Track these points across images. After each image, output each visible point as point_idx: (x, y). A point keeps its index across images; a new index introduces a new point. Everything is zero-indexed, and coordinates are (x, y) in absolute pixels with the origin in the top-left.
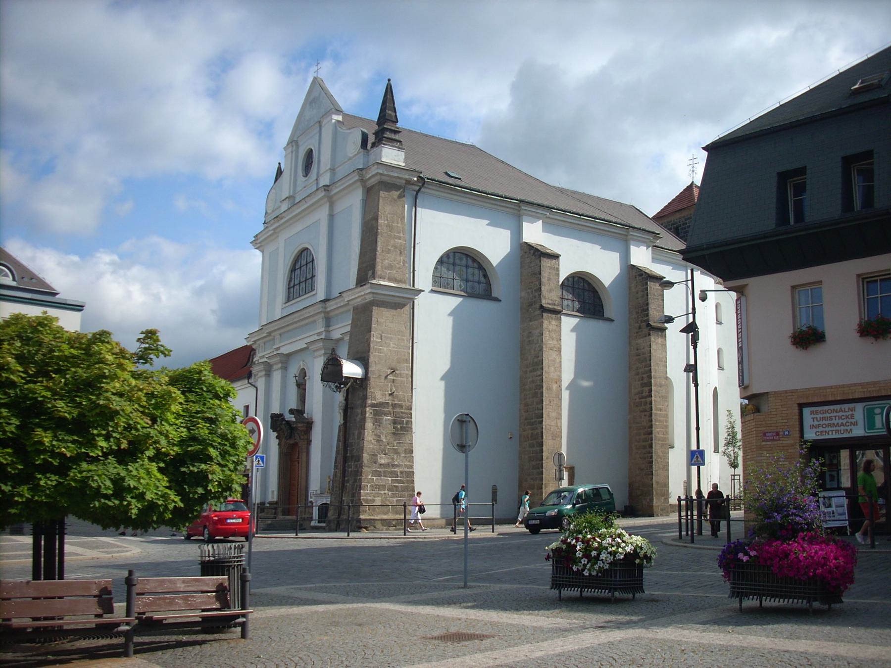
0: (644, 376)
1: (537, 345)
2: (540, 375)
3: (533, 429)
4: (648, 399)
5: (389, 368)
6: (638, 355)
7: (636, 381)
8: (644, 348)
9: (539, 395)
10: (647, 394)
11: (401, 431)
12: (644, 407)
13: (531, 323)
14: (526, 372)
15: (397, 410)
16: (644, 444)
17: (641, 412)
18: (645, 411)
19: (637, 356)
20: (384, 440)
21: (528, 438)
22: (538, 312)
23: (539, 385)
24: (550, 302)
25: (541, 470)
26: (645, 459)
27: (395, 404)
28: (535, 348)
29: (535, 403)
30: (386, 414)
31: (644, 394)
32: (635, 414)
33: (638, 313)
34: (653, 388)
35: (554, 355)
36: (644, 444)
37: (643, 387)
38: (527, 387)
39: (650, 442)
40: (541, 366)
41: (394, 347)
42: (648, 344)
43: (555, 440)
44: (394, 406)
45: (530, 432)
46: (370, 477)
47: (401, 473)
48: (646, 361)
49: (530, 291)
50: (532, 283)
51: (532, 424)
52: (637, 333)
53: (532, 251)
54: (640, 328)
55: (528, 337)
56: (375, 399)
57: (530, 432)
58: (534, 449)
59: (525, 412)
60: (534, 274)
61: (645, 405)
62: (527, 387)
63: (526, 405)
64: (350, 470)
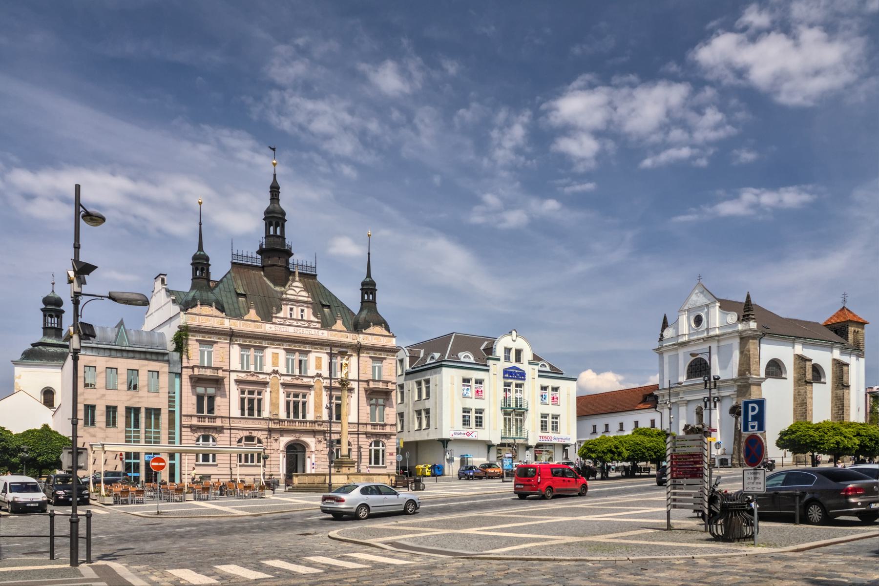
34: (845, 411)
35: (810, 400)
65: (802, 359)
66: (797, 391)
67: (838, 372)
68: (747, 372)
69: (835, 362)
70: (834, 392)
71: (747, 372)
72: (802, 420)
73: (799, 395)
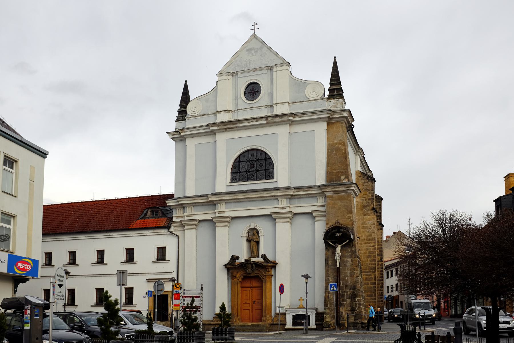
1: (370, 230)
2: (373, 246)
3: (368, 275)
9: (372, 257)
10: (379, 260)
13: (365, 217)
22: (372, 211)
23: (373, 252)
25: (374, 297)
29: (369, 261)
38: (362, 252)
39: (381, 285)
40: (374, 241)
42: (381, 234)
48: (379, 243)
49: (362, 198)
50: (366, 194)
51: (367, 272)
53: (366, 177)
55: (363, 224)
58: (368, 286)
60: (368, 190)
62: (362, 252)
65: (367, 178)
66: (360, 222)
68: (343, 177)
71: (343, 177)
72: (369, 262)
73: (364, 227)
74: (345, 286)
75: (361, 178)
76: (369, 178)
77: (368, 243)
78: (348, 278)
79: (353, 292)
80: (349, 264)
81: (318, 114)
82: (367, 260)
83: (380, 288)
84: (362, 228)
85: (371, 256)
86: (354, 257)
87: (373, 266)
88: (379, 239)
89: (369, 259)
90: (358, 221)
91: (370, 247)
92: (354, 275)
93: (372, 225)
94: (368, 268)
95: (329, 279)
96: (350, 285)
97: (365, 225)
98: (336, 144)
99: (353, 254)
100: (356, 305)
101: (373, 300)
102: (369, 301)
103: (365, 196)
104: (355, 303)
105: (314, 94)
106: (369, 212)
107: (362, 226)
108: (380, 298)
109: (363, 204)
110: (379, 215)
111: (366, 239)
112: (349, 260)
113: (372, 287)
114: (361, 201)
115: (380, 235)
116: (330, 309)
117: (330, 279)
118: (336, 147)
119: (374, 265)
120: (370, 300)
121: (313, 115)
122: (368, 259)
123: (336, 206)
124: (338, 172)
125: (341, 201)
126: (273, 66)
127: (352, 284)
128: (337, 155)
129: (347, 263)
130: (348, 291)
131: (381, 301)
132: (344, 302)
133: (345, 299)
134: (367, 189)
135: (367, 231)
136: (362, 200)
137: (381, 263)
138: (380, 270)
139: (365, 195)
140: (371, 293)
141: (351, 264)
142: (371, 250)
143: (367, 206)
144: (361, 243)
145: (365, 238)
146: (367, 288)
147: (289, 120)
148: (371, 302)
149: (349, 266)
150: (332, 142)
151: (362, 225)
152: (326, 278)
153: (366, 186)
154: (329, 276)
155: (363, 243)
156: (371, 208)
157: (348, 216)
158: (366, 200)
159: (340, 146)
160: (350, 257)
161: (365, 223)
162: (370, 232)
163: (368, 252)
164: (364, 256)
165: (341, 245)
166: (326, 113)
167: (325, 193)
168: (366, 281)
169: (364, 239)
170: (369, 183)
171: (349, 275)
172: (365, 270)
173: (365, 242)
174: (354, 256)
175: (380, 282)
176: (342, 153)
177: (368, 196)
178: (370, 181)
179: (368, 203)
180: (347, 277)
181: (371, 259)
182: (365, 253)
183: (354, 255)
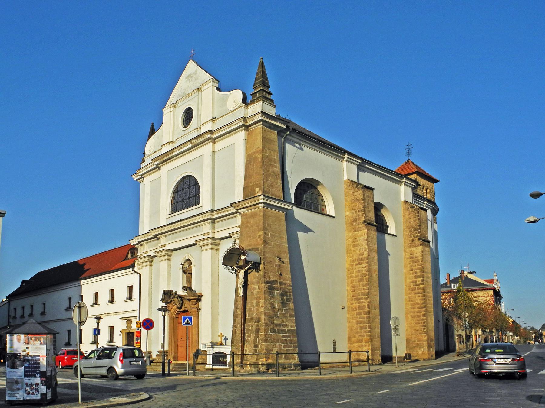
0: (417, 271)
1: (362, 247)
2: (365, 267)
4: (421, 286)
5: (276, 257)
6: (413, 258)
7: (410, 274)
8: (416, 254)
9: (365, 280)
11: (286, 301)
12: (418, 291)
13: (355, 233)
14: (352, 265)
15: (283, 286)
16: (418, 314)
17: (415, 294)
18: (418, 293)
19: (411, 258)
20: (276, 307)
21: (356, 308)
22: (363, 225)
23: (365, 274)
24: (370, 219)
26: (420, 323)
27: (282, 282)
28: (361, 249)
29: (361, 286)
30: (278, 289)
31: (417, 283)
32: (410, 295)
33: (411, 231)
36: (418, 314)
37: (417, 278)
38: (353, 275)
39: (423, 313)
41: (278, 242)
43: (376, 310)
44: (281, 284)
45: (357, 305)
46: (269, 333)
47: (288, 330)
48: (419, 262)
50: (356, 206)
51: (359, 299)
52: (410, 244)
53: (355, 185)
54: (413, 241)
55: (354, 242)
56: (270, 278)
57: (357, 305)
59: (352, 291)
60: (357, 200)
61: (418, 289)
62: (353, 275)
63: (353, 287)
64: (250, 328)
66: (351, 240)
67: (412, 220)
69: (407, 206)
70: (408, 250)
72: (361, 287)
73: (355, 245)
74: (251, 318)
75: (350, 188)
76: (359, 186)
77: (360, 264)
78: (254, 309)
79: (258, 326)
80: (255, 292)
81: (232, 124)
82: (360, 284)
83: (423, 316)
84: (353, 247)
85: (363, 280)
86: (261, 284)
87: (365, 291)
88: (418, 257)
89: (361, 283)
90: (349, 239)
91: (363, 269)
92: (259, 305)
93: (363, 241)
94: (360, 294)
95: (237, 310)
96: (256, 317)
97: (356, 243)
98: (254, 153)
99: (260, 279)
100: (259, 342)
101: (367, 333)
102: (362, 334)
103: (355, 208)
104: (259, 339)
105: (235, 104)
106: (360, 226)
107: (353, 243)
108: (422, 330)
109: (353, 218)
110: (418, 228)
111: (358, 260)
112: (257, 287)
113: (365, 317)
114: (351, 215)
115: (420, 252)
116: (236, 347)
117: (238, 310)
118: (254, 156)
119: (367, 290)
120: (363, 333)
121: (229, 126)
122: (361, 284)
123: (249, 225)
124: (253, 185)
125: (253, 218)
126: (201, 87)
127: (257, 316)
128: (254, 166)
129: (254, 290)
130: (253, 324)
131: (423, 332)
132: (248, 338)
133: (250, 334)
134: (357, 199)
135: (359, 249)
136: (352, 213)
137: (423, 286)
138: (421, 295)
139: (355, 207)
140: (364, 325)
141: (257, 291)
142: (364, 272)
143: (358, 220)
144: (352, 264)
145: (357, 258)
146: (360, 319)
147: (209, 139)
148: (364, 336)
149: (256, 294)
150: (250, 153)
151: (353, 242)
152: (235, 310)
153: (356, 196)
154: (237, 308)
155: (354, 264)
156: (362, 221)
157: (258, 234)
158: (356, 212)
159: (257, 154)
160: (257, 284)
161: (356, 240)
162: (361, 250)
163: (360, 275)
164: (355, 280)
165: (244, 270)
166: (239, 121)
167: (239, 211)
168: (358, 310)
169: (356, 260)
170: (359, 192)
171: (255, 306)
172: (357, 297)
173: (356, 263)
174: (261, 282)
175: (422, 309)
176: (259, 162)
177: (358, 207)
178: (360, 189)
179: (359, 215)
180: (253, 308)
181: (363, 283)
182: (357, 276)
183: (261, 280)
